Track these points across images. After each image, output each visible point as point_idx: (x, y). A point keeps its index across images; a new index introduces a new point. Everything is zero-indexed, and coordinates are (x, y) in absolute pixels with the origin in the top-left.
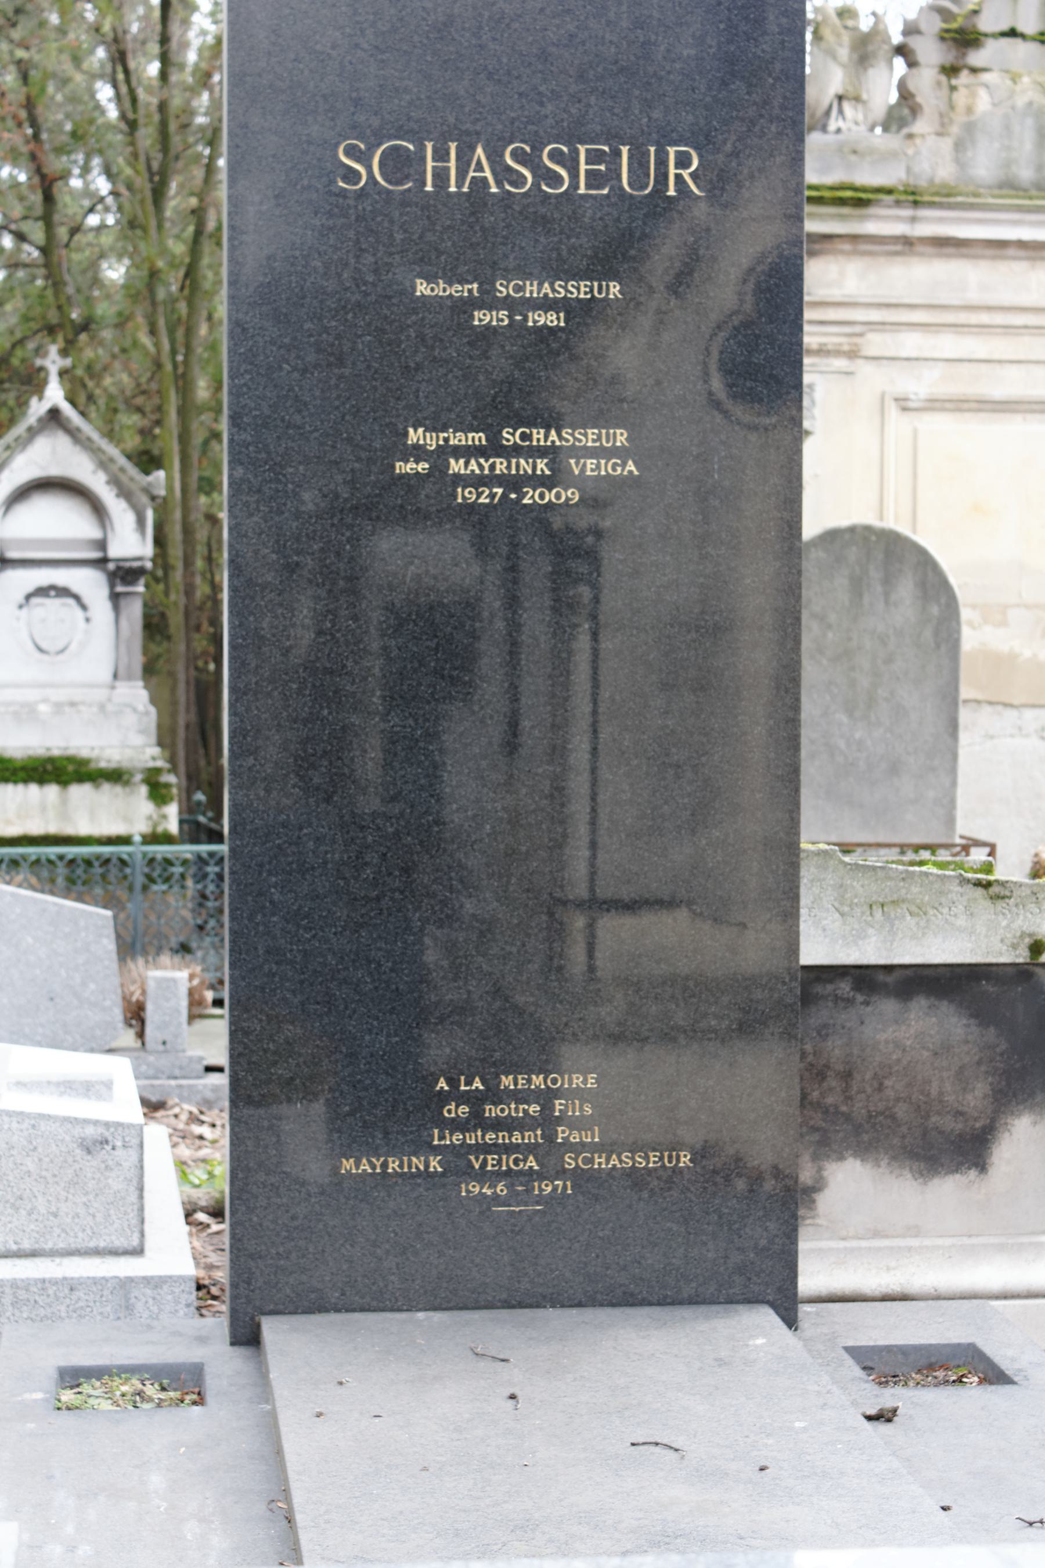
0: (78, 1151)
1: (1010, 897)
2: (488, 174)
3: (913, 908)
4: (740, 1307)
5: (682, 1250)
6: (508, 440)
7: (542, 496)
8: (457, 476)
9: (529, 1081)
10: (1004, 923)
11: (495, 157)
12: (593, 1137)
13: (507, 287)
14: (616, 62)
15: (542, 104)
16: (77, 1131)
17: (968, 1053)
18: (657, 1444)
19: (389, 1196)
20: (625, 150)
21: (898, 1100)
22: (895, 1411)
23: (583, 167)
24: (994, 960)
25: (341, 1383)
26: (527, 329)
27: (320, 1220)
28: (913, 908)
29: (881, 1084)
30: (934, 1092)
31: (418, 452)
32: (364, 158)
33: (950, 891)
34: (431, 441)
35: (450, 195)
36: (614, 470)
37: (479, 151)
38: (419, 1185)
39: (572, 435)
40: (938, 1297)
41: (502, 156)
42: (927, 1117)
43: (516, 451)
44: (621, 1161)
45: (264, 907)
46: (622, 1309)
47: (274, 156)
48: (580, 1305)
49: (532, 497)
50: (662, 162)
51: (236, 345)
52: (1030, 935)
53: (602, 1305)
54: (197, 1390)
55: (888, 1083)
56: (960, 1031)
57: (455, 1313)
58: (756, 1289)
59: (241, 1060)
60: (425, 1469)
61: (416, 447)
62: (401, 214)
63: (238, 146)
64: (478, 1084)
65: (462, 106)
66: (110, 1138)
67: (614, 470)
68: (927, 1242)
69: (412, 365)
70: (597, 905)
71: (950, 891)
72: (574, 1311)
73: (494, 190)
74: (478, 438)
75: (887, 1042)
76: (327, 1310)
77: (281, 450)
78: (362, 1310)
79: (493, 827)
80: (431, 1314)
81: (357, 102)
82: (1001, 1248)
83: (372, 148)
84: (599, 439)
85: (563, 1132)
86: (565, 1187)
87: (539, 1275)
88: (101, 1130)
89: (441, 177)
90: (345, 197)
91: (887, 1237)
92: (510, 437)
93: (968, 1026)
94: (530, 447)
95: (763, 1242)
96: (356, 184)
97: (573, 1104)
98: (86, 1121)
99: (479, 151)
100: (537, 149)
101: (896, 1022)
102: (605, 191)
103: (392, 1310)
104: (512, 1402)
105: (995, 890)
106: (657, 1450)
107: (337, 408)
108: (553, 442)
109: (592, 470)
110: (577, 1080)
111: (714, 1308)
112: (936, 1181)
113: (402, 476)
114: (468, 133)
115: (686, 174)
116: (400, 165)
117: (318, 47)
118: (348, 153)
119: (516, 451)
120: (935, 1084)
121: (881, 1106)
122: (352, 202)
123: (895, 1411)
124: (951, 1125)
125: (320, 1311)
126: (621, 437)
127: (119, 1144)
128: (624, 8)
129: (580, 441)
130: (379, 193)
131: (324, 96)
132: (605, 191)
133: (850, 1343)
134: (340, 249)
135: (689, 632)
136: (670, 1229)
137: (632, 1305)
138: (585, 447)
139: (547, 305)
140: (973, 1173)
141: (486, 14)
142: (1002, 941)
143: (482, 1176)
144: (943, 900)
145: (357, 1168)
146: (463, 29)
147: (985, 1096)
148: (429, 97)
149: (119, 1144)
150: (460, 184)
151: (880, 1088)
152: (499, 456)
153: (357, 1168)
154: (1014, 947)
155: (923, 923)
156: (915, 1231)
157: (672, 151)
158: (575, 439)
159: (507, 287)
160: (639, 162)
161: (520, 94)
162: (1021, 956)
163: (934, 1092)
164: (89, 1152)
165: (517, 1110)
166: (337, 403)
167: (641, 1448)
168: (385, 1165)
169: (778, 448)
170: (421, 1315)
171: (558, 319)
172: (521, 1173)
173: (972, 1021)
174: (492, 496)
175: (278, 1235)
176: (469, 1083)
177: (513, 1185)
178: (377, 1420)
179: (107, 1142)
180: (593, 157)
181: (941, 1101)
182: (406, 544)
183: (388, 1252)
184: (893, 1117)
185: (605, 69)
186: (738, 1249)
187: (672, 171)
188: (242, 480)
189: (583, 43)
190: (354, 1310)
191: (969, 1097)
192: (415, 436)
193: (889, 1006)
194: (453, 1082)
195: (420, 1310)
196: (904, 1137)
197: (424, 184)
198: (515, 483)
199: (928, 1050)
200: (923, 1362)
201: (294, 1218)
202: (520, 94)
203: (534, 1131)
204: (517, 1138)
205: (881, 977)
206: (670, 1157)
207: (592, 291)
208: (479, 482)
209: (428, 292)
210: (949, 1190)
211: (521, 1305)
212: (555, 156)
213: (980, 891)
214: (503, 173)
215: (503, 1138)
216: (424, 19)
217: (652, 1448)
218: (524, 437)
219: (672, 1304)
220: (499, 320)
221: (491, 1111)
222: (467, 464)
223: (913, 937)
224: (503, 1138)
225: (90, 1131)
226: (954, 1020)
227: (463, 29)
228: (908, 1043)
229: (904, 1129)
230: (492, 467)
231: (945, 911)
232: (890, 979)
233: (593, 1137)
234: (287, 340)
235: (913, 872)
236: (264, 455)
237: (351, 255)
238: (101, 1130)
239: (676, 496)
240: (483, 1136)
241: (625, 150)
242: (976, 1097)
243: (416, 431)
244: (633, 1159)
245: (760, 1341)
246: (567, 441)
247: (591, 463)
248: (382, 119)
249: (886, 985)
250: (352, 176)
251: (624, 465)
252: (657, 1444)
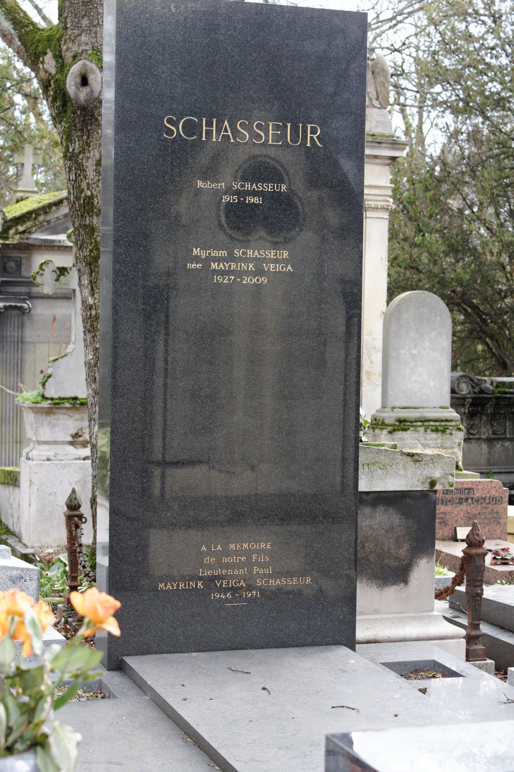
0: (9, 582)
1: (421, 461)
2: (230, 133)
3: (381, 466)
4: (332, 647)
5: (306, 622)
6: (237, 254)
7: (251, 280)
8: (214, 270)
9: (242, 546)
10: (419, 472)
11: (233, 125)
12: (269, 571)
13: (237, 185)
14: (286, 85)
15: (254, 103)
16: (9, 573)
17: (400, 531)
18: (343, 707)
19: (180, 600)
20: (289, 125)
21: (371, 552)
22: (426, 689)
23: (271, 132)
24: (415, 489)
25: (183, 685)
26: (246, 204)
27: (149, 612)
28: (381, 466)
29: (364, 545)
30: (386, 549)
31: (197, 259)
32: (176, 124)
33: (397, 458)
34: (203, 254)
35: (213, 142)
36: (283, 269)
37: (226, 123)
38: (193, 595)
39: (265, 253)
40: (390, 641)
41: (236, 125)
42: (383, 560)
44: (281, 582)
45: (125, 467)
46: (281, 649)
47: (135, 122)
48: (262, 648)
49: (247, 280)
50: (305, 132)
51: (117, 208)
52: (430, 478)
53: (272, 647)
54: (99, 692)
55: (366, 545)
56: (397, 521)
57: (209, 653)
58: (338, 638)
59: (114, 538)
60: (251, 721)
61: (197, 257)
62: (191, 151)
63: (119, 117)
64: (219, 548)
65: (219, 102)
66: (24, 576)
67: (283, 269)
68: (383, 616)
69: (195, 219)
70: (164, 464)
71: (397, 458)
72: (261, 650)
73: (232, 141)
74: (224, 253)
75: (366, 526)
76: (151, 653)
77: (137, 257)
78: (167, 653)
79: (228, 431)
80: (198, 653)
81: (173, 98)
82: (414, 618)
83: (179, 120)
84: (276, 255)
85: (256, 569)
86: (257, 594)
87: (245, 635)
88: (20, 572)
90: (167, 142)
91: (365, 614)
92: (238, 253)
93: (400, 519)
94: (247, 258)
95: (341, 617)
96: (172, 136)
97: (261, 556)
98: (13, 568)
99: (226, 123)
100: (251, 123)
101: (370, 517)
102: (280, 143)
103: (180, 652)
104: (265, 691)
105: (416, 457)
106: (344, 709)
107: (162, 238)
108: (256, 256)
109: (273, 269)
110: (263, 545)
111: (321, 647)
112: (386, 589)
113: (190, 270)
114: (221, 115)
115: (315, 137)
117: (156, 72)
118: (168, 122)
120: (386, 545)
121: (363, 555)
122: (170, 144)
123: (426, 689)
124: (393, 563)
125: (148, 654)
126: (286, 254)
127: (28, 578)
128: (290, 61)
129: (268, 255)
130: (182, 141)
131: (158, 95)
132: (280, 143)
133: (382, 662)
134: (164, 165)
135: (313, 342)
136: (302, 612)
137: (285, 647)
138: (270, 258)
139: (254, 193)
140: (402, 585)
141: (230, 61)
142: (418, 480)
143: (221, 590)
144: (394, 462)
145: (166, 587)
146: (220, 67)
147: (408, 550)
148: (204, 98)
149: (28, 578)
150: (217, 139)
152: (233, 262)
153: (166, 587)
154: (423, 483)
155: (385, 473)
156: (377, 611)
157: (309, 126)
158: (266, 254)
159: (237, 185)
161: (244, 98)
162: (426, 487)
163: (386, 549)
164: (14, 583)
165: (236, 559)
166: (162, 236)
167: (337, 709)
168: (178, 585)
169: (352, 261)
170: (193, 654)
171: (259, 200)
172: (238, 587)
173: (402, 517)
174: (229, 280)
175: (130, 619)
176: (215, 547)
177: (234, 594)
178: (212, 701)
179: (22, 578)
181: (389, 553)
182: (192, 301)
183: (179, 625)
184: (369, 561)
185: (281, 88)
186: (331, 621)
187: (309, 135)
188: (119, 270)
189: (272, 76)
190: (163, 653)
191: (401, 551)
192: (196, 251)
193: (367, 510)
194: (209, 548)
195: (192, 652)
196: (373, 569)
197: (202, 137)
199: (384, 529)
200: (413, 669)
201: (137, 611)
202: (244, 98)
203: (243, 569)
204: (236, 572)
205: (364, 497)
206: (302, 579)
207: (274, 188)
209: (203, 186)
210: (392, 592)
211: (236, 649)
212: (259, 126)
213: (409, 458)
215: (230, 572)
216: (203, 62)
217: (342, 709)
218: (244, 253)
219: (302, 646)
220: (233, 200)
221: (225, 560)
222: (218, 265)
223: (381, 479)
225: (15, 573)
226: (395, 516)
227: (220, 67)
228: (375, 527)
229: (373, 566)
230: (230, 266)
231: (395, 467)
232: (368, 498)
233: (269, 571)
234: (140, 207)
235: (382, 450)
236: (129, 259)
237: (169, 168)
238: (20, 572)
239: (309, 281)
240: (221, 571)
241: (289, 125)
242: (404, 551)
243: (196, 250)
244: (286, 581)
245: (352, 661)
246: (262, 255)
247: (272, 266)
248: (184, 107)
249: (366, 500)
250: (170, 132)
251: (287, 267)
252: (343, 707)
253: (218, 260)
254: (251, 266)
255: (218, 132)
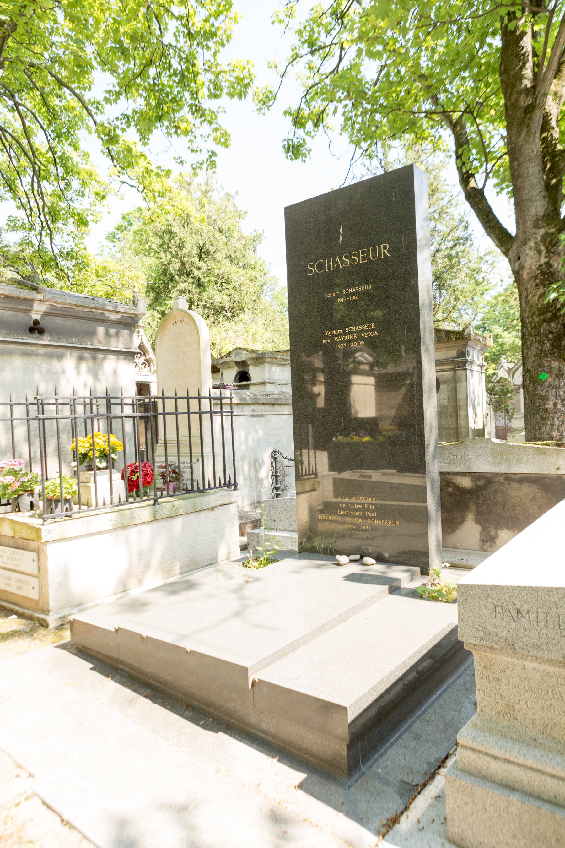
11: (341, 259)
31: (328, 337)
32: (314, 267)
43: (349, 333)
50: (380, 250)
61: (327, 336)
74: (340, 331)
89: (329, 267)
92: (347, 330)
116: (321, 266)
119: (349, 333)
139: (354, 294)
151: (514, 510)
160: (374, 251)
180: (363, 252)
198: (349, 342)
204: (357, 514)
208: (340, 342)
212: (355, 255)
214: (343, 262)
224: (353, 513)
247: (366, 334)
253: (338, 336)
254: (355, 336)
255: (334, 265)
